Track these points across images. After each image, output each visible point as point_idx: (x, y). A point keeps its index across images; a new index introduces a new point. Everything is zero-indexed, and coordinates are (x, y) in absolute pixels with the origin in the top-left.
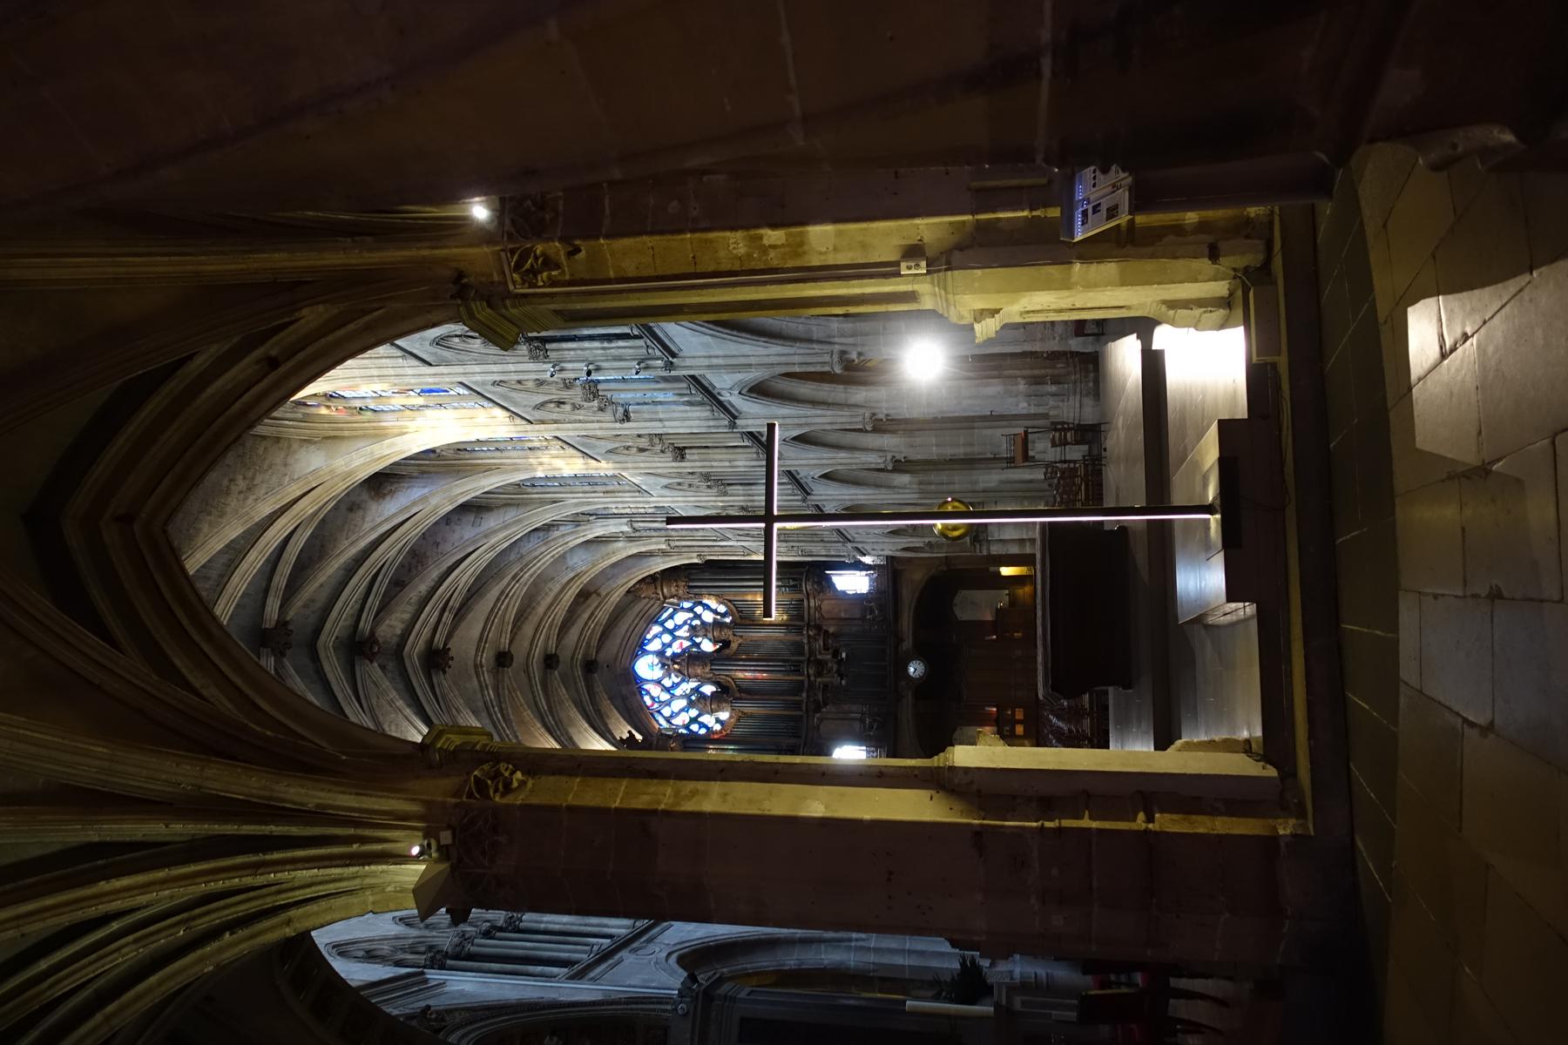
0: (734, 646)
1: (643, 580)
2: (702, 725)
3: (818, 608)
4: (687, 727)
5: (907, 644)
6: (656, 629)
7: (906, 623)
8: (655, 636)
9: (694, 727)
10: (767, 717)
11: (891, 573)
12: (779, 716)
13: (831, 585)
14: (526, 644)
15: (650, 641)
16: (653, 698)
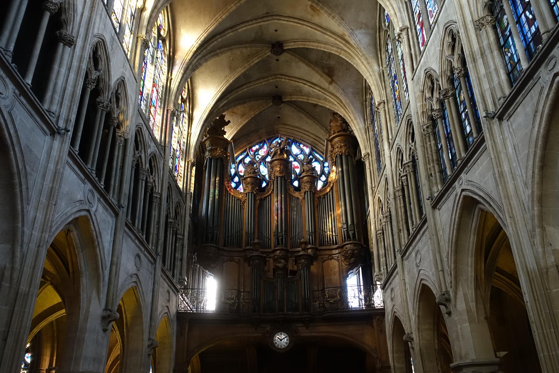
0: (297, 194)
1: (344, 121)
2: (238, 184)
3: (331, 257)
4: (237, 174)
5: (304, 332)
6: (307, 150)
7: (323, 330)
8: (302, 151)
9: (236, 179)
10: (241, 220)
11: (370, 316)
12: (242, 229)
13: (351, 267)
14: (289, 12)
15: (298, 147)
16: (257, 150)
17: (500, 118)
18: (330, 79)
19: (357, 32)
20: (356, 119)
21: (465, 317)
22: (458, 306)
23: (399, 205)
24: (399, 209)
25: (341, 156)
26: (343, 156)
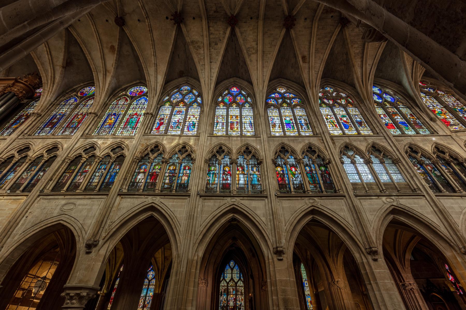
14: (100, 31)
17: (201, 196)
18: (65, 66)
19: (115, 79)
20: (54, 94)
21: (102, 259)
22: (100, 251)
23: (62, 167)
24: (61, 169)
25: (14, 95)
26: (15, 97)
